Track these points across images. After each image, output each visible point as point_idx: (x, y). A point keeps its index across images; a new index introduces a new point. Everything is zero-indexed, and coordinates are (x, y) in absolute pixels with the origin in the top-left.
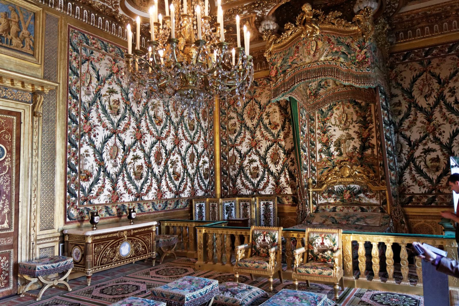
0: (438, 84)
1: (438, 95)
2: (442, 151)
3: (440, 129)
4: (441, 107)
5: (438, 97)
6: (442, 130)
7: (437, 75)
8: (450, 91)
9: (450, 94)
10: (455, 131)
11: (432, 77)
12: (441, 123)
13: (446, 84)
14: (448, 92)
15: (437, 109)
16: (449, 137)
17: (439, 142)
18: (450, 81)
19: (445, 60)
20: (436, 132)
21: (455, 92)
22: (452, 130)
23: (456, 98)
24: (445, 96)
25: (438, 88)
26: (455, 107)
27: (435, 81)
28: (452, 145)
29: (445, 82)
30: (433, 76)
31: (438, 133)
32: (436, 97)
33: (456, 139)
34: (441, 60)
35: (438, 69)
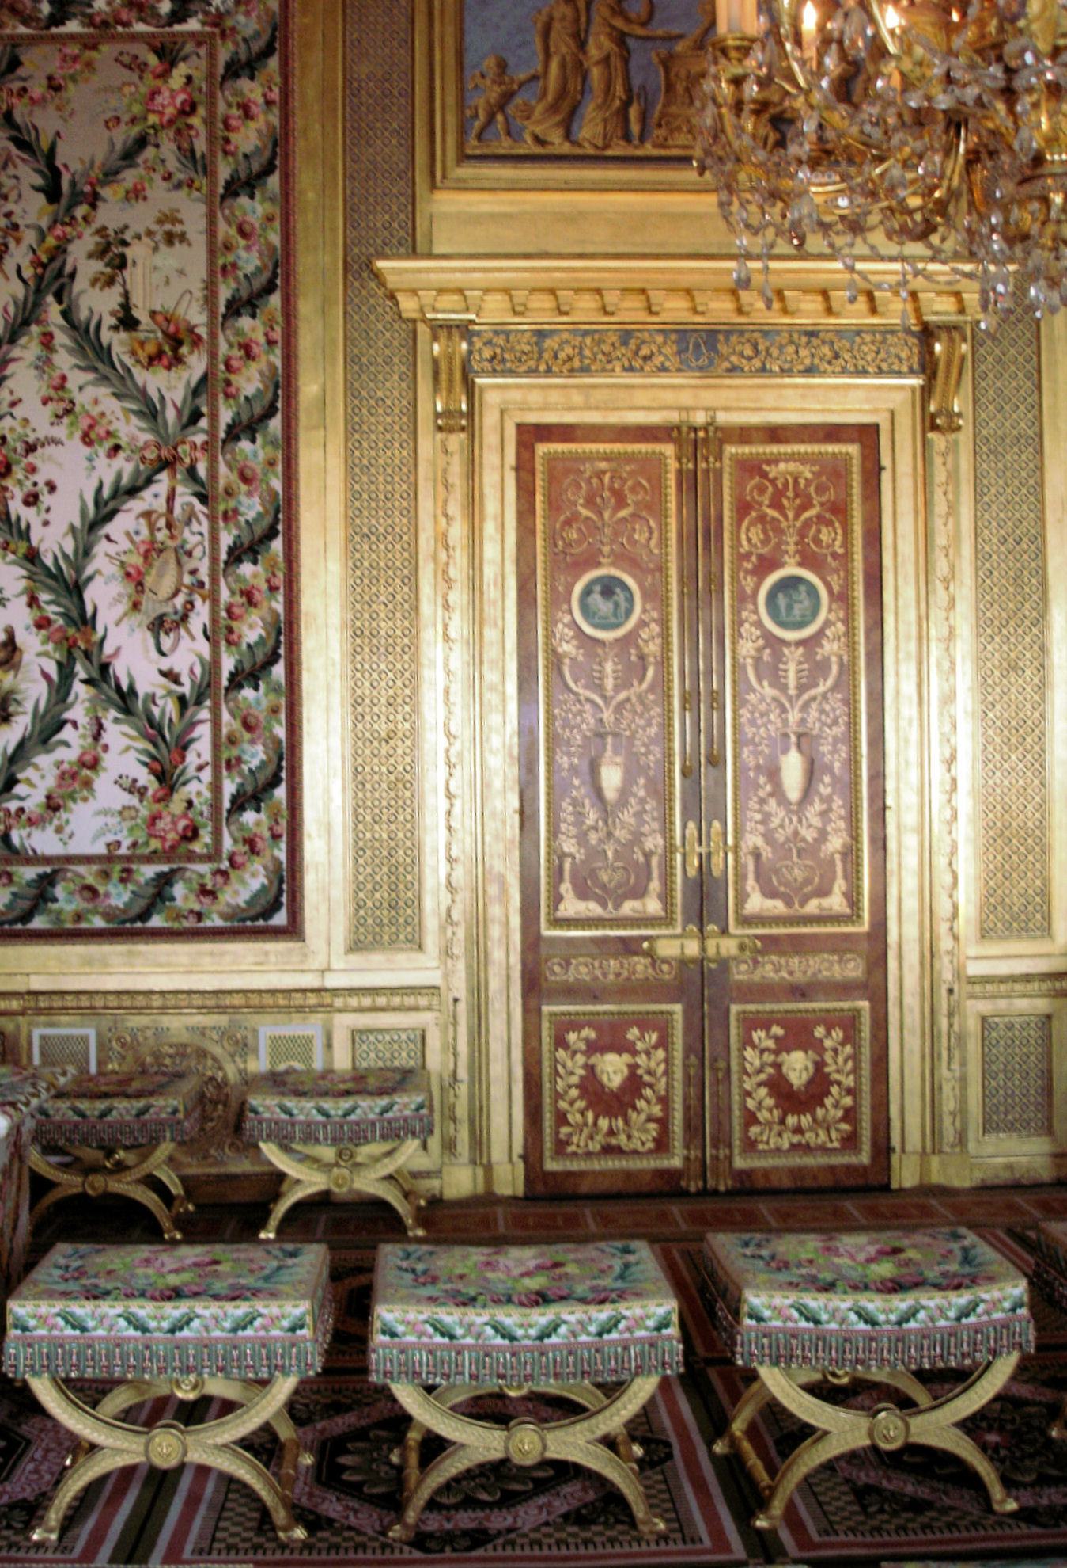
0: (41, 199)
1: (37, 263)
2: (33, 601)
3: (32, 469)
4: (47, 340)
5: (39, 278)
6: (40, 478)
7: (45, 145)
8: (101, 252)
9: (98, 266)
10: (106, 493)
11: (14, 151)
12: (41, 435)
13: (80, 211)
14: (90, 256)
15: (28, 350)
16: (78, 523)
17: (23, 548)
18: (105, 192)
19: (89, 65)
20: (9, 483)
21: (123, 257)
22: (96, 484)
23: (126, 295)
24: (72, 275)
25: (44, 223)
26: (116, 350)
27: (29, 175)
28: (88, 571)
29: (77, 197)
30: (23, 144)
31: (19, 495)
32: (28, 273)
33: (108, 538)
34: (75, 59)
35: (51, 109)
